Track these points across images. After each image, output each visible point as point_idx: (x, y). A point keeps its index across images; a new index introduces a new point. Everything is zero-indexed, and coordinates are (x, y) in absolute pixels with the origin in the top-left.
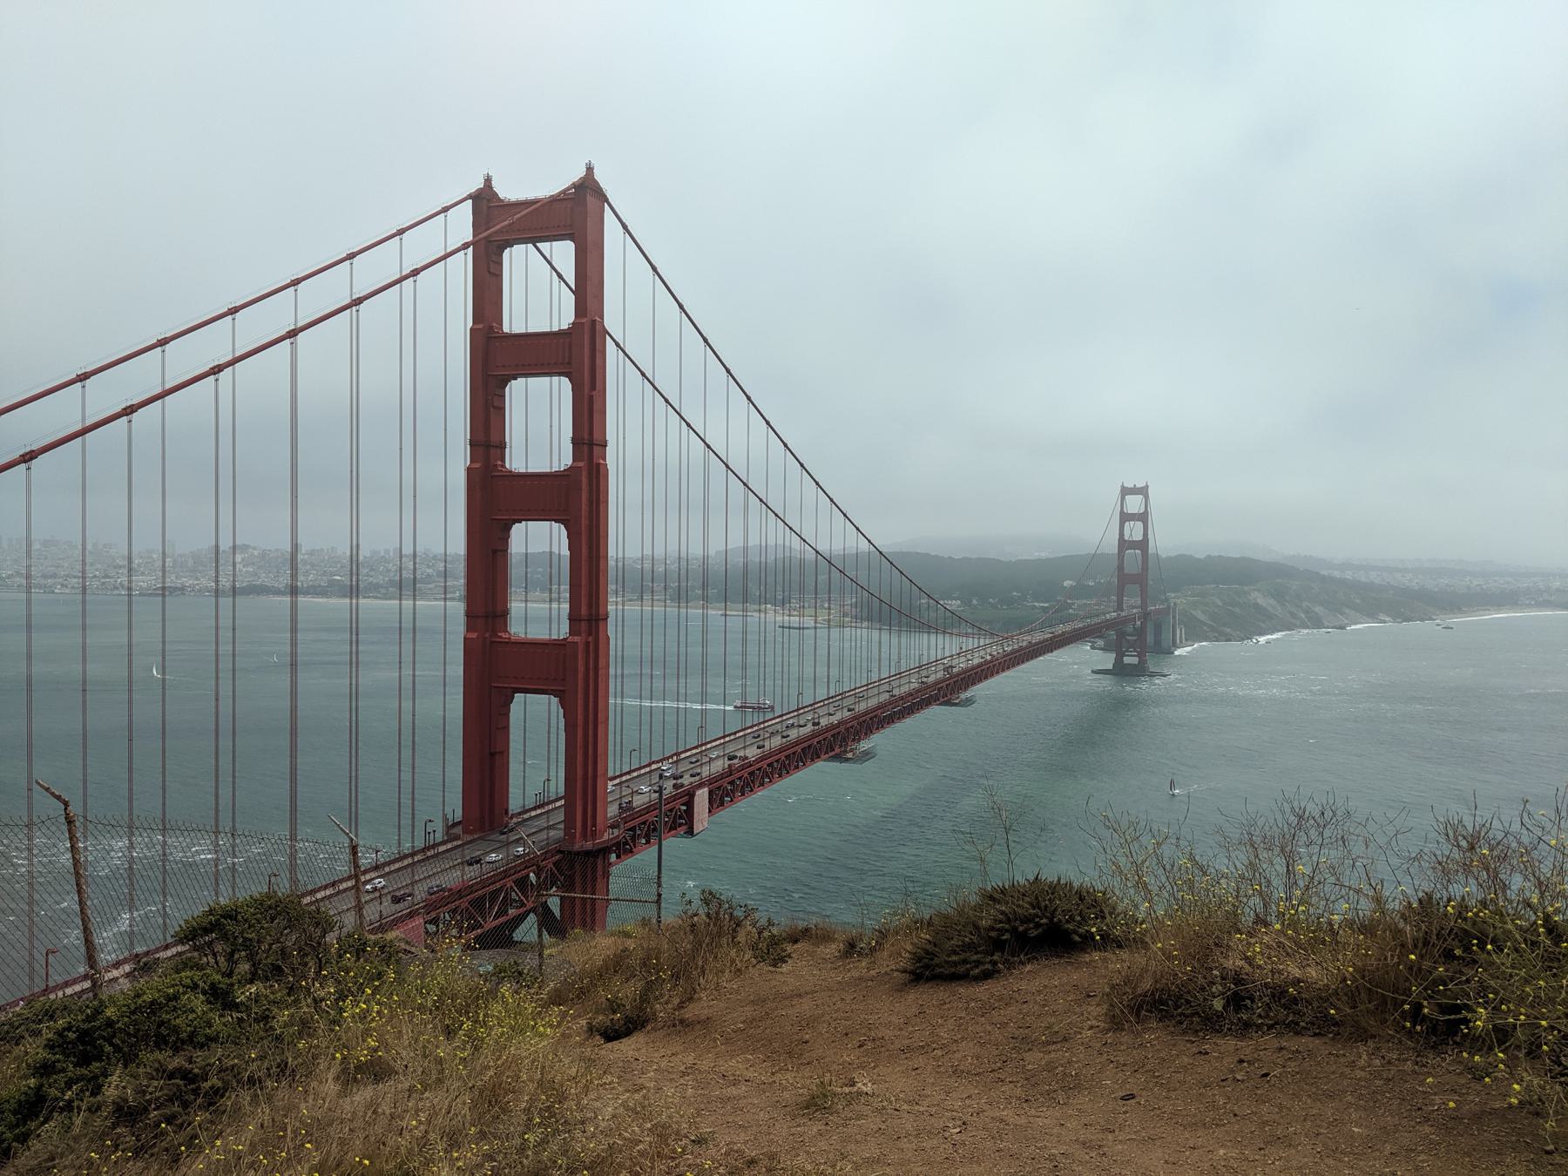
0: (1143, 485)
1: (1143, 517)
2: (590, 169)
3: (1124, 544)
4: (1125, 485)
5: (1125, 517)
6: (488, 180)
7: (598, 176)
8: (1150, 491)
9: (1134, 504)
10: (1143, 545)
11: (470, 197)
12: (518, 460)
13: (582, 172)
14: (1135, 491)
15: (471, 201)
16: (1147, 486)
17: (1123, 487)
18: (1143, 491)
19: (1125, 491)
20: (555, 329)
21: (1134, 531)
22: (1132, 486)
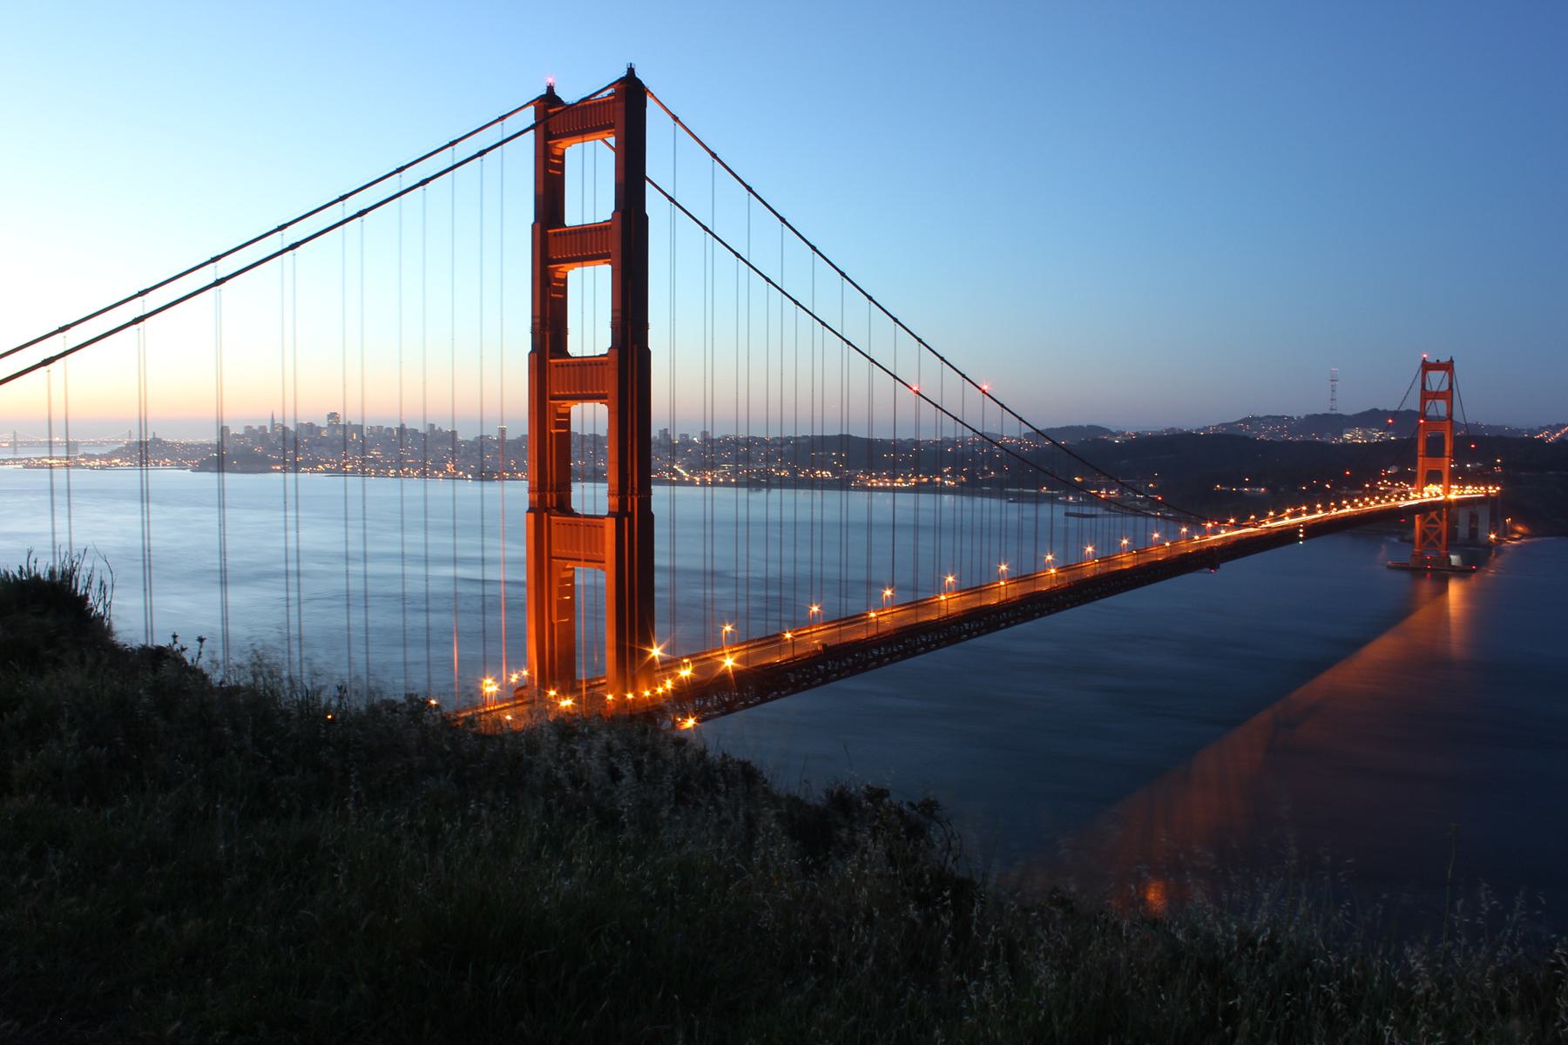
0: (1448, 359)
1: (1448, 395)
2: (631, 71)
5: (1426, 395)
6: (550, 89)
7: (639, 74)
8: (1455, 365)
9: (1437, 380)
11: (528, 104)
13: (623, 73)
14: (1438, 366)
15: (532, 108)
16: (1452, 361)
18: (1448, 367)
19: (1426, 367)
20: (599, 220)
22: (1432, 360)
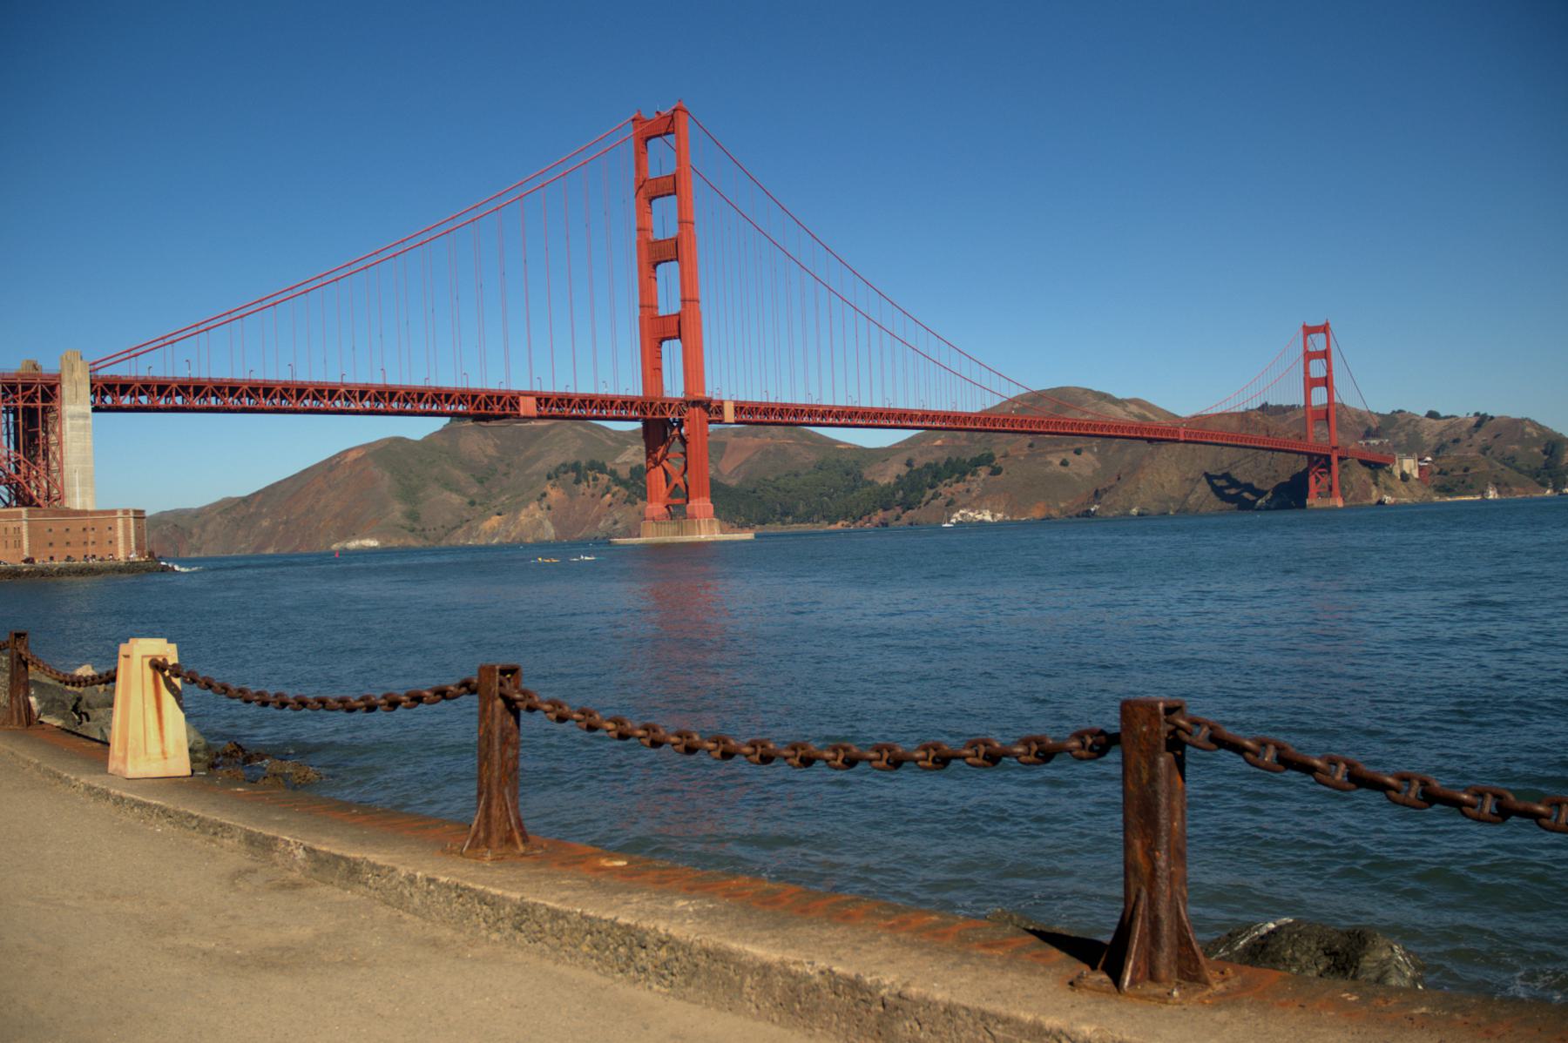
0: (1321, 322)
1: (1326, 355)
3: (1310, 383)
4: (1307, 324)
5: (1309, 356)
8: (1331, 326)
9: (1318, 341)
10: (1326, 382)
12: (658, 235)
14: (1315, 330)
15: (631, 124)
16: (1327, 324)
17: (1304, 327)
18: (1325, 329)
19: (1308, 331)
21: (1318, 369)
